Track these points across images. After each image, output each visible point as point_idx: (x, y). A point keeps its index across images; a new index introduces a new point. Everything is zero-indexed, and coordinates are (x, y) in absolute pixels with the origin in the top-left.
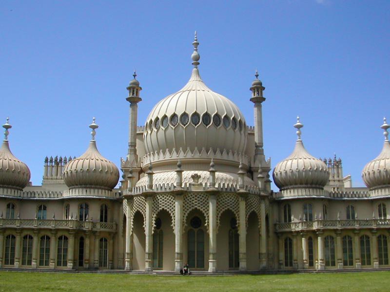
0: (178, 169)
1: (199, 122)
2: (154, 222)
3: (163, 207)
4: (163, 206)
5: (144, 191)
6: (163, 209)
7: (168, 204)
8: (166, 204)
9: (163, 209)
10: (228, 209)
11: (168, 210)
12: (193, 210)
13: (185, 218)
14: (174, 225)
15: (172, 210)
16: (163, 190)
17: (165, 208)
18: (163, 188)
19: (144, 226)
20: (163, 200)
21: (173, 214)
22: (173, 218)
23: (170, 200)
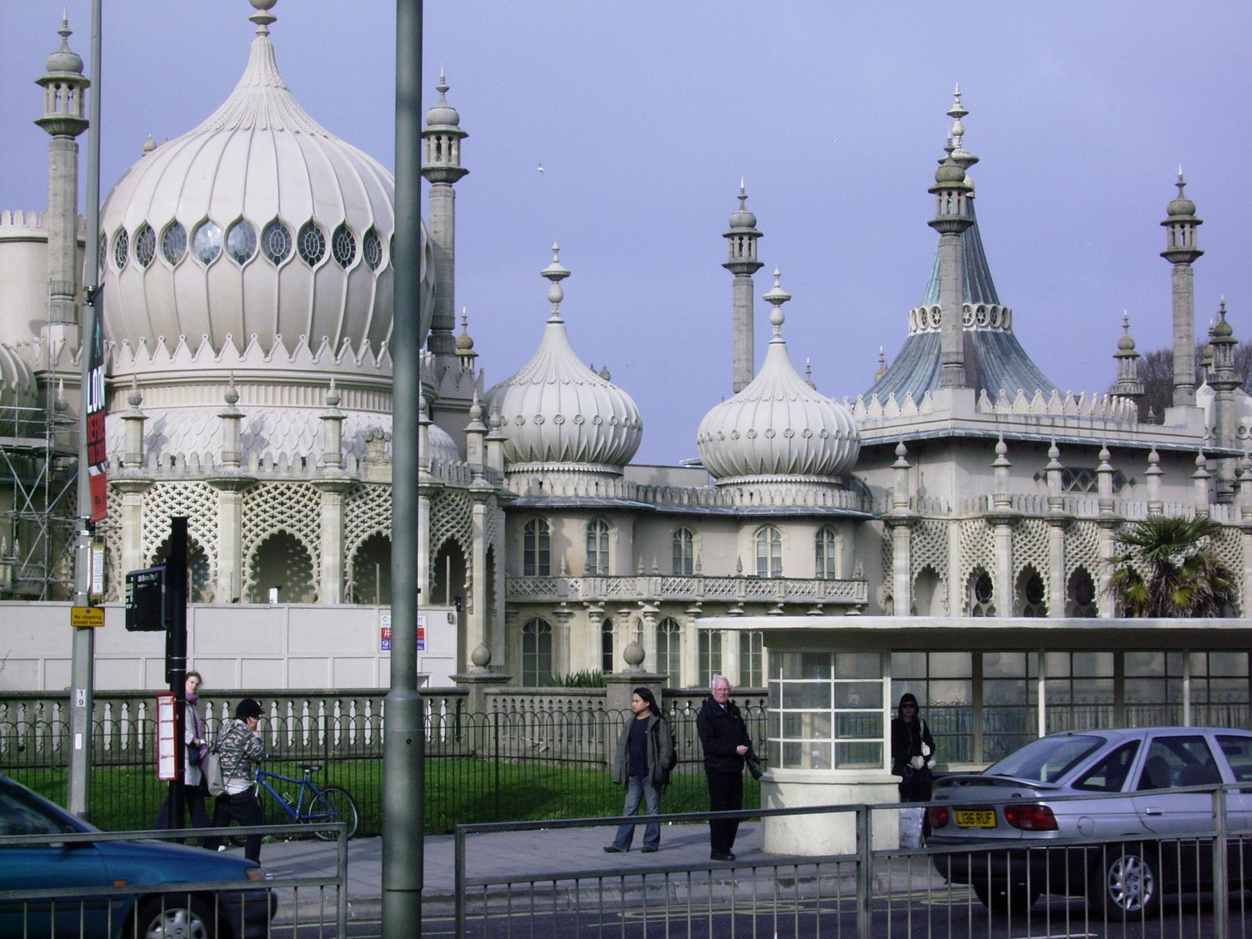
0: (332, 412)
1: (322, 252)
2: (249, 571)
3: (280, 526)
4: (282, 522)
5: (209, 472)
6: (282, 532)
7: (298, 516)
8: (292, 517)
9: (282, 532)
10: (453, 536)
11: (298, 536)
12: (371, 537)
13: (349, 561)
14: (319, 582)
15: (312, 536)
16: (284, 475)
17: (289, 530)
18: (283, 466)
19: (210, 582)
20: (282, 504)
21: (316, 549)
22: (314, 561)
23: (306, 506)
